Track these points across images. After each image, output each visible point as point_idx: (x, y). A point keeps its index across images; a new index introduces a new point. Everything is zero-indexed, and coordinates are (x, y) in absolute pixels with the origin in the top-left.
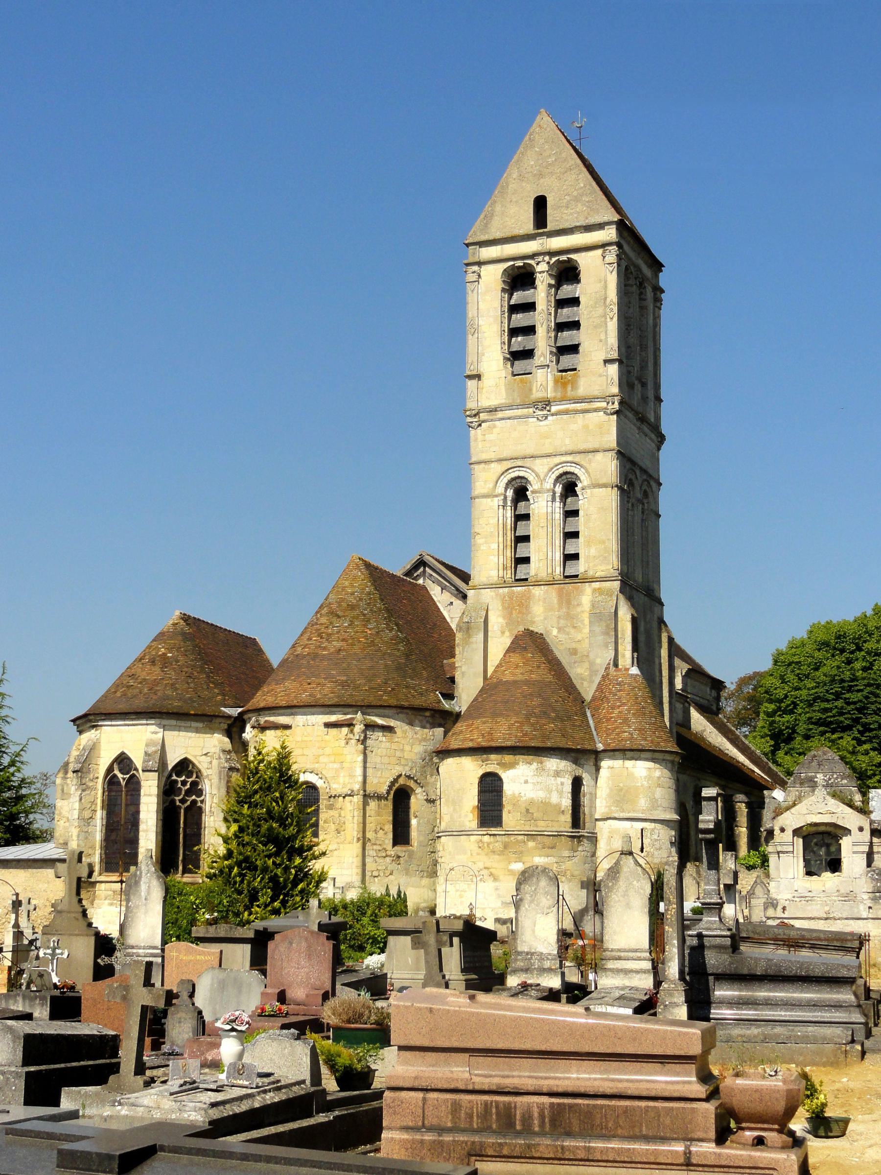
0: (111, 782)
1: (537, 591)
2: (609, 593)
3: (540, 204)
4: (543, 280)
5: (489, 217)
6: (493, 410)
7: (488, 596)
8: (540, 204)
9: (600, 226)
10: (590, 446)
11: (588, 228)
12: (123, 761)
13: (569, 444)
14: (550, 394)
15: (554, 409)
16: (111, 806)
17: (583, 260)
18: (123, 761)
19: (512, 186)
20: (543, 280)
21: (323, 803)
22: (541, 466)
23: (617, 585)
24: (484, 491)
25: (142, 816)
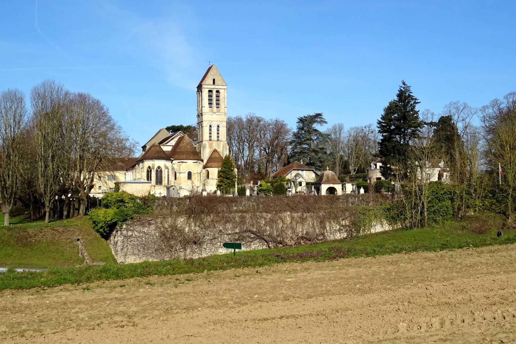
0: (157, 171)
1: (214, 142)
2: (225, 144)
3: (214, 80)
4: (214, 93)
5: (205, 82)
6: (206, 113)
7: (206, 142)
8: (214, 80)
9: (224, 86)
10: (222, 120)
11: (222, 86)
12: (159, 167)
13: (219, 120)
14: (216, 111)
15: (217, 113)
16: (157, 174)
17: (221, 91)
18: (159, 167)
19: (209, 76)
20: (214, 93)
21: (192, 174)
22: (215, 123)
23: (226, 142)
24: (206, 125)
25: (163, 176)
